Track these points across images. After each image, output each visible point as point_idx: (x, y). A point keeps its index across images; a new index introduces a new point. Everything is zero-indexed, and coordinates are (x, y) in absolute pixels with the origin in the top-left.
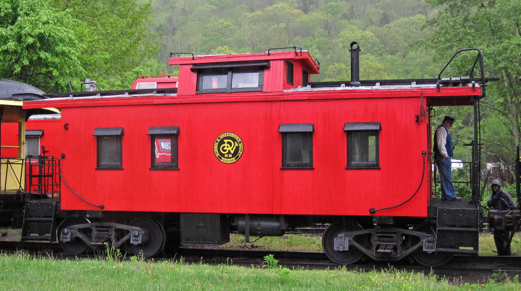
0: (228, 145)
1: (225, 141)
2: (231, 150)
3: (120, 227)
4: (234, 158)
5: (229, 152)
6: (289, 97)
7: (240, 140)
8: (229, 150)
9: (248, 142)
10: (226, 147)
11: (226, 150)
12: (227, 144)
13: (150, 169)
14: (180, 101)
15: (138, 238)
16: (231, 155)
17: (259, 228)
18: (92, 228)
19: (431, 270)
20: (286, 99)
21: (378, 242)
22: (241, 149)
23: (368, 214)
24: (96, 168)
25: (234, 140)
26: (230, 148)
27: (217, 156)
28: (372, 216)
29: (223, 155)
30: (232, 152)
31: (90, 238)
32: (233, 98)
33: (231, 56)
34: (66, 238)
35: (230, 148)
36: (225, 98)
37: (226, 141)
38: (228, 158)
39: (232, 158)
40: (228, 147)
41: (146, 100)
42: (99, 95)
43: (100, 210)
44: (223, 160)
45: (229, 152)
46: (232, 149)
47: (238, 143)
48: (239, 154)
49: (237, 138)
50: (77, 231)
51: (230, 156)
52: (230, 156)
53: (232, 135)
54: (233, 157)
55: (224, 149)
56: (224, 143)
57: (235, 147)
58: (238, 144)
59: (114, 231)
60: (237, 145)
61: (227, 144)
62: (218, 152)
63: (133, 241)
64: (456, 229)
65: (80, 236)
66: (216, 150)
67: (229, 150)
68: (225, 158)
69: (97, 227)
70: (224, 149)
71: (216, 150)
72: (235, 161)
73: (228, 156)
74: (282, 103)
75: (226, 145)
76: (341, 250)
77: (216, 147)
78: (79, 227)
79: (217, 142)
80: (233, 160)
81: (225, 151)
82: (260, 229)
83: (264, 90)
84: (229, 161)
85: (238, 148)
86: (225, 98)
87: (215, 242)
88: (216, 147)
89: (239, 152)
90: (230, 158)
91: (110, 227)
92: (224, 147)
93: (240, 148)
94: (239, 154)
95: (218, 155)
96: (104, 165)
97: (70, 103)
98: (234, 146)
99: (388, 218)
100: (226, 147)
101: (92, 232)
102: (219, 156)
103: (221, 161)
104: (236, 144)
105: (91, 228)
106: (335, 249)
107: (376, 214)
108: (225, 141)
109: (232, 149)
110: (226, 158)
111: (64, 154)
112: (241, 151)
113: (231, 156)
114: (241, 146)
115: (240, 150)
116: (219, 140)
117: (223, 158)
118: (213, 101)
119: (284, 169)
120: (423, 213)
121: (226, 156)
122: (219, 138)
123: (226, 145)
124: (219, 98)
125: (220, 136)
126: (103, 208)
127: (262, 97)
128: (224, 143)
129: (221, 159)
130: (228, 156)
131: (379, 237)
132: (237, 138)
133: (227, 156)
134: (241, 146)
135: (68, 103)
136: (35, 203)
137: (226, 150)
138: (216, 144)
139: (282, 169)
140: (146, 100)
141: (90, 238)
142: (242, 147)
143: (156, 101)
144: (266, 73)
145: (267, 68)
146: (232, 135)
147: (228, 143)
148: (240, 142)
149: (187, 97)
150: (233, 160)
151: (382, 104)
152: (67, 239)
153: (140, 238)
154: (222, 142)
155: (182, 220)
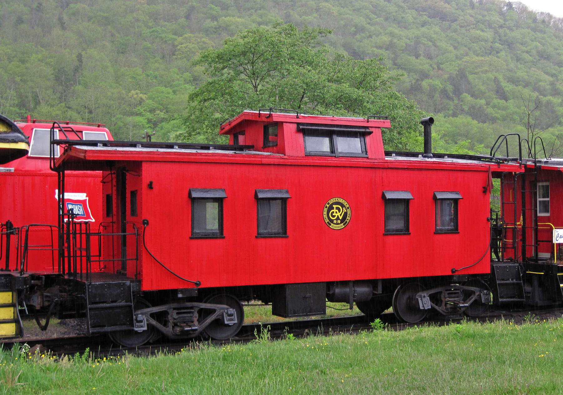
0: (337, 211)
1: (333, 206)
2: (339, 216)
3: (205, 306)
4: (342, 224)
6: (392, 165)
7: (348, 206)
8: (338, 216)
9: (355, 208)
10: (335, 212)
11: (335, 216)
12: (336, 209)
13: (256, 236)
14: (291, 162)
15: (233, 317)
17: (356, 295)
18: (170, 311)
19: (502, 317)
20: (389, 166)
21: (448, 299)
22: (349, 215)
23: (450, 274)
24: (190, 236)
25: (343, 206)
26: (339, 214)
27: (326, 222)
28: (453, 275)
29: (332, 221)
30: (341, 218)
31: (165, 324)
32: (343, 162)
33: (335, 119)
34: (142, 327)
35: (339, 214)
36: (336, 162)
37: (335, 206)
38: (337, 224)
39: (341, 224)
40: (336, 213)
41: (254, 159)
42: (140, 146)
43: (196, 288)
44: (333, 226)
46: (341, 215)
47: (346, 209)
48: (347, 220)
49: (345, 203)
50: (149, 317)
51: (339, 222)
53: (341, 200)
54: (341, 223)
55: (333, 214)
56: (333, 208)
57: (343, 213)
58: (346, 210)
59: (197, 311)
60: (345, 211)
61: (336, 209)
62: (327, 218)
63: (227, 321)
64: (108, 305)
65: (154, 322)
66: (325, 216)
67: (338, 216)
68: (334, 224)
69: (174, 309)
70: (333, 214)
71: (325, 216)
72: (344, 227)
73: (337, 222)
74: (384, 171)
75: (335, 210)
76: (426, 308)
77: (325, 213)
78: (152, 311)
79: (326, 207)
80: (342, 226)
81: (334, 216)
82: (357, 296)
83: (369, 155)
84: (336, 227)
85: (346, 214)
86: (336, 162)
87: (299, 313)
88: (325, 213)
89: (348, 218)
91: (192, 308)
92: (333, 212)
93: (348, 214)
94: (347, 220)
95: (327, 221)
96: (198, 233)
97: (157, 156)
98: (342, 212)
99: (464, 276)
100: (335, 212)
101: (169, 316)
102: (328, 222)
103: (330, 227)
104: (344, 210)
105: (168, 310)
106: (421, 308)
107: (456, 274)
108: (333, 206)
110: (335, 224)
111: (147, 220)
112: (349, 217)
113: (339, 222)
114: (349, 212)
115: (348, 216)
116: (328, 206)
117: (332, 224)
118: (324, 164)
119: (387, 235)
120: (488, 271)
122: (328, 204)
123: (335, 210)
124: (330, 162)
125: (330, 201)
126: (200, 284)
127: (369, 163)
128: (333, 208)
129: (330, 225)
130: (337, 222)
131: (449, 294)
132: (345, 203)
133: (336, 222)
134: (349, 212)
135: (155, 156)
136: (99, 284)
137: (335, 216)
138: (326, 210)
139: (384, 235)
140: (254, 159)
141: (165, 324)
143: (265, 161)
144: (368, 139)
145: (370, 133)
146: (341, 200)
147: (337, 208)
148: (348, 208)
149: (298, 158)
150: (342, 226)
151: (460, 174)
152: (144, 327)
153: (235, 316)
154: (331, 208)
155: (288, 292)
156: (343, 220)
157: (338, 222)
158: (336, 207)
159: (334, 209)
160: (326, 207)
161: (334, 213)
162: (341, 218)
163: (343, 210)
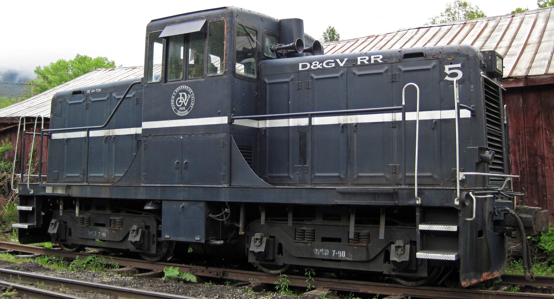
0: (183, 98)
1: (179, 94)
5: (183, 105)
8: (183, 102)
10: (181, 100)
16: (185, 108)
25: (188, 93)
29: (178, 108)
30: (186, 105)
37: (181, 94)
40: (182, 100)
45: (183, 105)
52: (184, 108)
54: (186, 109)
57: (188, 99)
67: (183, 102)
72: (188, 113)
81: (179, 104)
85: (190, 100)
90: (184, 111)
92: (179, 100)
98: (187, 98)
100: (181, 100)
102: (175, 110)
103: (177, 114)
104: (189, 96)
108: (179, 94)
109: (186, 102)
110: (181, 111)
117: (178, 111)
121: (180, 109)
123: (181, 98)
129: (177, 112)
142: (193, 98)
147: (183, 96)
156: (187, 108)
157: (183, 109)
158: (182, 94)
159: (180, 97)
161: (180, 101)
162: (186, 105)
163: (187, 96)
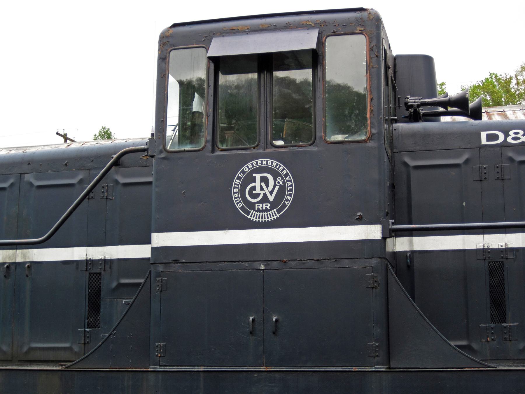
2: (268, 195)
4: (275, 210)
5: (265, 199)
29: (252, 206)
30: (271, 198)
40: (262, 189)
45: (265, 199)
46: (271, 193)
47: (282, 178)
48: (287, 200)
61: (261, 181)
73: (262, 207)
85: (282, 189)
117: (252, 211)
130: (262, 207)
134: (291, 184)
137: (259, 195)
142: (291, 186)
148: (286, 175)
160: (239, 178)
162: (271, 198)
